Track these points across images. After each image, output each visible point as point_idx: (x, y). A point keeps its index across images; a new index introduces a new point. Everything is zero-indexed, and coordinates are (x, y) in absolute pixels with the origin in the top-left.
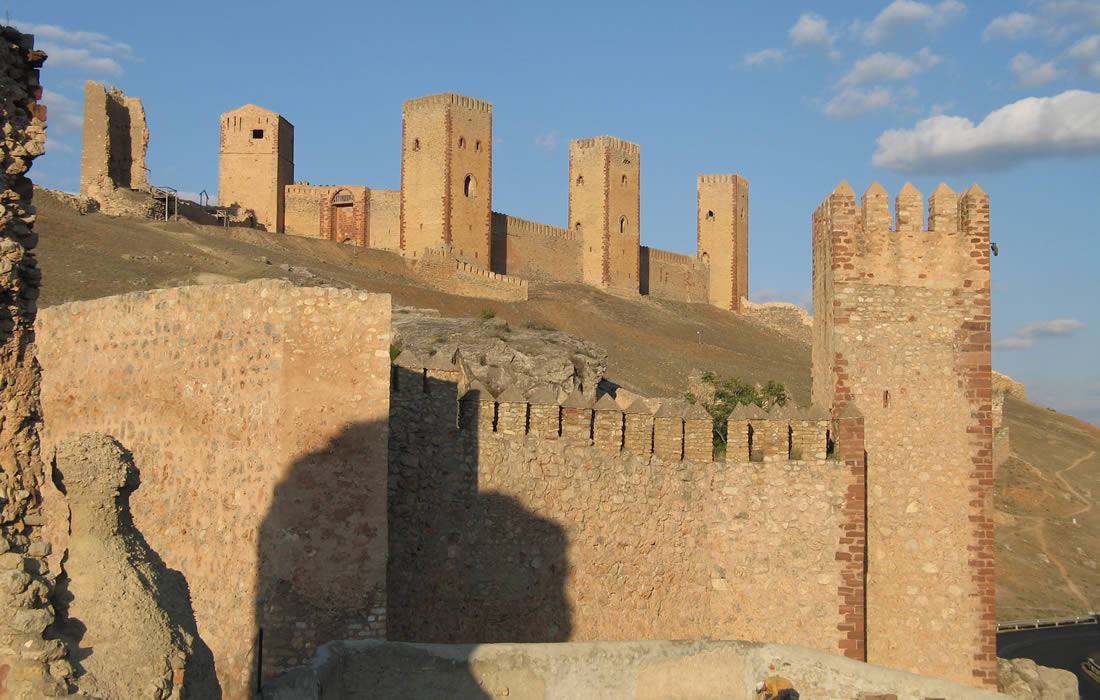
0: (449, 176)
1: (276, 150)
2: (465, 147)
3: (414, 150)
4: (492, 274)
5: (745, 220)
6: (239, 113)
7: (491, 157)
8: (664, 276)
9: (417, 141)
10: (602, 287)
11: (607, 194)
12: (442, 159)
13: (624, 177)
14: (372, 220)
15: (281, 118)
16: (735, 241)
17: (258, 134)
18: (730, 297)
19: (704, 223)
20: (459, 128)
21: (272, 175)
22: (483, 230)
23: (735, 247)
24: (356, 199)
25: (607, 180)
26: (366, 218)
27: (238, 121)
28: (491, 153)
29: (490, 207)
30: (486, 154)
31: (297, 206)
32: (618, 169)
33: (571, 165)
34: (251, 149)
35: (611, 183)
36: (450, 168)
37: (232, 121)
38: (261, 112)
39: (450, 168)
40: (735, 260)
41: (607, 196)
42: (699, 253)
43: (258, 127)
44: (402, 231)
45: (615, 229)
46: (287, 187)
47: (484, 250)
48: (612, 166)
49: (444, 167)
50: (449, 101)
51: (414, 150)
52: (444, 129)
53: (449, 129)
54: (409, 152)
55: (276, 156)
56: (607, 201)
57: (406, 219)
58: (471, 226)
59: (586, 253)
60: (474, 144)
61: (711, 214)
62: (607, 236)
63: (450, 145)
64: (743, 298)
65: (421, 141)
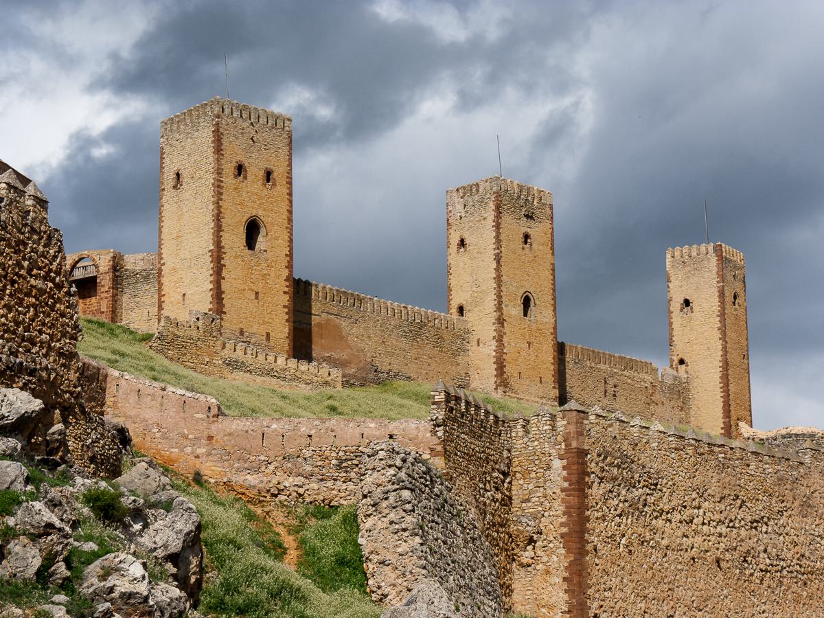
0: (218, 219)
2: (245, 178)
3: (175, 187)
4: (293, 363)
5: (741, 312)
7: (290, 194)
8: (611, 390)
9: (178, 175)
10: (498, 396)
11: (498, 258)
12: (209, 194)
13: (526, 237)
14: (125, 299)
16: (724, 338)
18: (720, 423)
19: (677, 318)
20: (235, 151)
22: (281, 298)
23: (725, 349)
24: (101, 269)
25: (497, 237)
26: (114, 296)
28: (290, 188)
29: (290, 266)
30: (281, 190)
32: (514, 226)
33: (448, 224)
35: (504, 244)
36: (219, 207)
39: (219, 207)
40: (726, 366)
41: (498, 262)
42: (672, 361)
45: (514, 310)
47: (281, 330)
48: (507, 219)
49: (211, 207)
50: (217, 109)
52: (209, 151)
53: (218, 150)
54: (168, 195)
56: (498, 269)
57: (165, 290)
58: (257, 293)
59: (473, 348)
60: (262, 173)
61: (687, 303)
62: (501, 321)
64: (742, 424)
65: (184, 174)
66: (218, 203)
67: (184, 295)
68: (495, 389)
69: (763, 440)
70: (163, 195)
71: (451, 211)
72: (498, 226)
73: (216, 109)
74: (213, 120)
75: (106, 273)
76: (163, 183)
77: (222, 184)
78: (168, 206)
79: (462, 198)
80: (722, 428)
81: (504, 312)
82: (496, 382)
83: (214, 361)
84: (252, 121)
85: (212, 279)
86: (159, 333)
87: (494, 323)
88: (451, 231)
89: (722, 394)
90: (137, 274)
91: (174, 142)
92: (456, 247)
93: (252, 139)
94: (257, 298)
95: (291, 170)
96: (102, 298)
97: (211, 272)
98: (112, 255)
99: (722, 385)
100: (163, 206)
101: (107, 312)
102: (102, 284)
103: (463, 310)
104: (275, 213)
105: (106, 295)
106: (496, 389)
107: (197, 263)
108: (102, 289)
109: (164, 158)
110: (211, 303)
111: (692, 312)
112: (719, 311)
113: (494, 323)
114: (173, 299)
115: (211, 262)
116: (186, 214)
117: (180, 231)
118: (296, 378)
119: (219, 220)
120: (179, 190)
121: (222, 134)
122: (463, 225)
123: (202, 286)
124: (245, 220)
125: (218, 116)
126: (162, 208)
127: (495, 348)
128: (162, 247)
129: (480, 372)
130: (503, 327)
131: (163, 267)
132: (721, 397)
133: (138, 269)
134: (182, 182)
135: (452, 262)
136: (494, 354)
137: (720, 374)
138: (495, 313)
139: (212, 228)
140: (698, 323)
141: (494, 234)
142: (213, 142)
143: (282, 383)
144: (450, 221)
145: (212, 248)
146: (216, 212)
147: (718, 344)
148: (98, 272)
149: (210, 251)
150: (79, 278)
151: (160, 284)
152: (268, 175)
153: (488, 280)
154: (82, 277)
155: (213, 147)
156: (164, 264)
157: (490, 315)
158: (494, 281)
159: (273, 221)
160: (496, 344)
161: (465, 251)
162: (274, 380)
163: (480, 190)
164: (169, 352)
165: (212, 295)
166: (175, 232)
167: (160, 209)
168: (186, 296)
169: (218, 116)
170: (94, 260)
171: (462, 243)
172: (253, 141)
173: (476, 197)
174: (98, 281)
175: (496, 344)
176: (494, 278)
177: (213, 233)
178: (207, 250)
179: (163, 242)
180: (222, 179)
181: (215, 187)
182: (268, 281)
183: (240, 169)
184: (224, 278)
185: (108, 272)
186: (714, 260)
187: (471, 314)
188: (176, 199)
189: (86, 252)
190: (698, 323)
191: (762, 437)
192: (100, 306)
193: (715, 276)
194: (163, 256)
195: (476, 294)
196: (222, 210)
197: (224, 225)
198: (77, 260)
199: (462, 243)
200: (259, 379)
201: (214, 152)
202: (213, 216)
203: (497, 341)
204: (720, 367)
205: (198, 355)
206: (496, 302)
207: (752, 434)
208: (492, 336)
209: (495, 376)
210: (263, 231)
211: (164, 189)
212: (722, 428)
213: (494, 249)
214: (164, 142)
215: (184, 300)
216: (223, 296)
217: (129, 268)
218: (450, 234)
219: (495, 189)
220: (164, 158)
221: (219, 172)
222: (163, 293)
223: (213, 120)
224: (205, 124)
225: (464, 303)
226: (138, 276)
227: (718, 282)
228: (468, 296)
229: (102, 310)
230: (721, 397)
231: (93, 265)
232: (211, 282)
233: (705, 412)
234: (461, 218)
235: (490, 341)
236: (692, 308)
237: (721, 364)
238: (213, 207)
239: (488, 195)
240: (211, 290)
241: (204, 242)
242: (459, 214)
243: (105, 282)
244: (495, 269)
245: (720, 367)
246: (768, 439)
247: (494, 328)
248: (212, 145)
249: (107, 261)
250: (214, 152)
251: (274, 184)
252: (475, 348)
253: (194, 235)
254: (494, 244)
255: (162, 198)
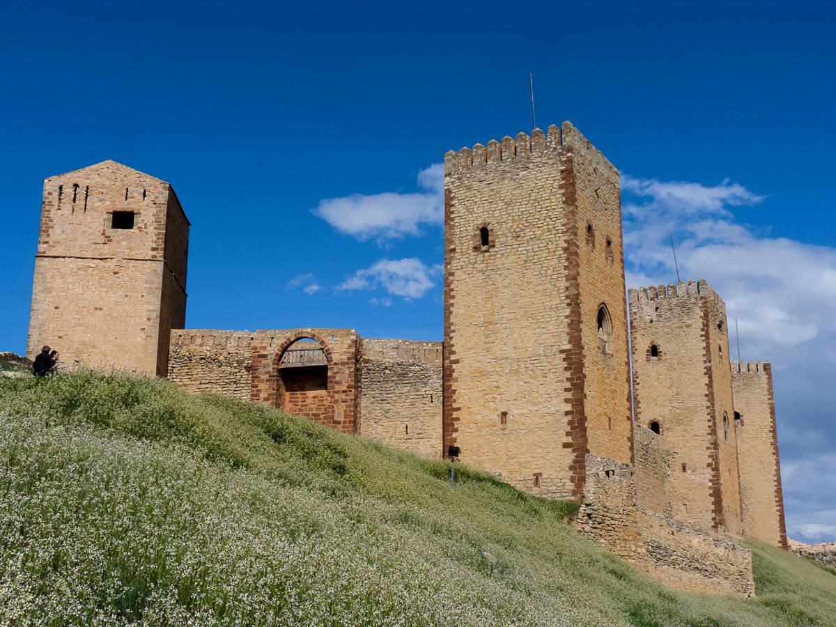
0: (574, 302)
1: (161, 253)
2: (594, 245)
3: (476, 248)
6: (82, 176)
9: (484, 234)
11: (709, 372)
12: (557, 262)
14: (364, 402)
15: (171, 189)
17: (123, 220)
21: (152, 304)
24: (336, 357)
25: (707, 348)
27: (81, 192)
31: (197, 372)
34: (106, 250)
37: (68, 191)
38: (131, 176)
41: (710, 377)
43: (122, 206)
44: (449, 425)
46: (175, 332)
49: (563, 284)
51: (476, 248)
52: (557, 200)
53: (570, 199)
55: (159, 267)
56: (710, 385)
57: (460, 400)
62: (715, 445)
63: (576, 234)
66: (576, 279)
67: (504, 414)
68: (712, 526)
69: (813, 554)
70: (451, 258)
71: (635, 313)
72: (707, 336)
73: (567, 139)
74: (560, 154)
75: (343, 364)
76: (451, 242)
77: (578, 251)
78: (464, 276)
79: (652, 299)
80: (779, 542)
81: (718, 435)
82: (714, 519)
83: (639, 550)
84: (594, 165)
85: (569, 395)
86: (587, 505)
87: (708, 448)
88: (636, 335)
89: (778, 508)
90: (386, 368)
91: (475, 184)
92: (646, 354)
93: (596, 191)
94: (610, 429)
95: (622, 242)
96: (338, 401)
97: (568, 385)
98: (354, 337)
99: (777, 499)
100: (452, 274)
101: (345, 422)
102: (337, 378)
103: (659, 428)
104: (616, 301)
105: (343, 396)
106: (715, 527)
107: (531, 367)
108: (337, 388)
109: (453, 205)
110: (568, 434)
111: (743, 425)
112: (772, 427)
113: (708, 448)
114: (478, 417)
115: (566, 369)
116: (506, 290)
117: (492, 314)
118: (716, 571)
119: (578, 304)
120: (488, 254)
121: (575, 175)
122: (654, 330)
123: (546, 404)
124: (596, 308)
125: (570, 150)
126: (451, 278)
127: (711, 478)
128: (452, 335)
129: (688, 504)
130: (718, 452)
131: (454, 366)
132: (777, 511)
133: (388, 361)
134: (493, 241)
135: (639, 370)
136: (710, 484)
137: (775, 488)
138: (709, 436)
139: (566, 317)
140: (749, 436)
141: (704, 344)
142: (561, 187)
143: (706, 580)
144: (635, 324)
145: (569, 347)
146: (576, 292)
147: (771, 458)
148: (330, 360)
149: (562, 352)
150: (293, 366)
151: (447, 393)
152: (609, 243)
153: (697, 396)
154: (300, 365)
155: (563, 194)
156: (457, 362)
157: (701, 438)
158: (706, 398)
159: (614, 309)
160: (713, 473)
161: (661, 359)
162: (697, 575)
163: (679, 293)
164: (602, 540)
165: (570, 423)
166: (480, 314)
167: (446, 279)
168: (509, 417)
169: (570, 150)
170: (322, 343)
171: (654, 351)
172: (597, 195)
173: (674, 301)
174: (330, 374)
175: (713, 473)
176: (706, 395)
177: (568, 324)
178: (555, 349)
179: (453, 328)
180: (578, 243)
181: (571, 254)
182: (616, 401)
183: (589, 228)
184: (585, 396)
185: (347, 363)
186: (764, 377)
187: (670, 433)
188: (480, 266)
189: (309, 330)
190: (749, 436)
191: (812, 552)
192: (333, 412)
193: (766, 393)
194: (453, 349)
195: (678, 411)
196: (580, 290)
197: (582, 312)
198: (293, 339)
199: (654, 351)
200: (686, 575)
201: (564, 202)
202: (567, 297)
203: (713, 470)
204: (775, 481)
205: (626, 541)
206: (711, 423)
207: (800, 547)
208: (706, 463)
209: (713, 511)
210: (606, 324)
211: (454, 250)
212: (779, 542)
213: (705, 362)
214: (452, 183)
215: (503, 422)
216: (586, 425)
217: (372, 358)
218: (635, 338)
219: (702, 294)
220: (453, 205)
221: (573, 231)
222: (455, 405)
223: (560, 154)
224: (544, 159)
225: (660, 419)
226: (387, 371)
227: (769, 399)
228: (666, 411)
229: (336, 419)
230: (777, 511)
231: (322, 349)
232: (567, 401)
233: (760, 523)
234: (651, 322)
235: (703, 468)
236: (742, 422)
237: (775, 478)
238: (567, 284)
239: (693, 300)
240: (567, 413)
241: (548, 336)
242: (648, 319)
243: (342, 377)
244: (706, 384)
245: (775, 481)
246: (818, 554)
247: (708, 453)
248: (563, 191)
249: (347, 346)
250: (564, 202)
251: (613, 261)
252: (678, 472)
253: (525, 323)
254: (704, 355)
255: (450, 263)
